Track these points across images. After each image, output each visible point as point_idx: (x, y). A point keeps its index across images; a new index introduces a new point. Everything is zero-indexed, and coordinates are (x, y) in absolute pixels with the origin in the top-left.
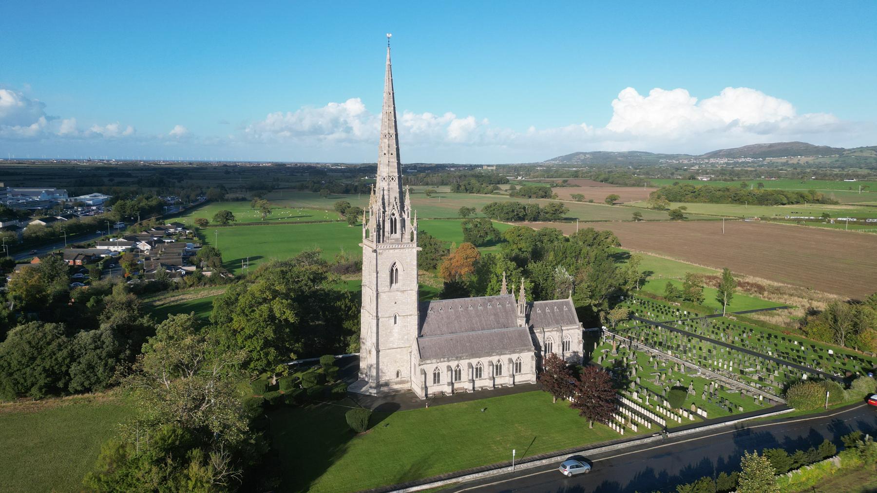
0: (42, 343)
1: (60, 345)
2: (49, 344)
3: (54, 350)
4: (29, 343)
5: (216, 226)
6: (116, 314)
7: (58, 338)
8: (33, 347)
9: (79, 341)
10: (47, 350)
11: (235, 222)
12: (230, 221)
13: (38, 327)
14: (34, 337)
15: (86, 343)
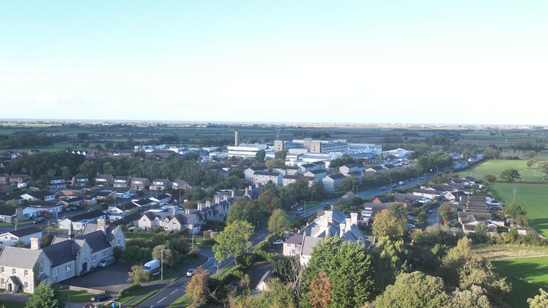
0: (427, 295)
1: (442, 301)
2: (432, 297)
3: (437, 305)
4: (417, 292)
5: (502, 182)
6: (475, 272)
7: (440, 293)
8: (420, 298)
9: (457, 301)
10: (431, 303)
11: (519, 180)
12: (515, 179)
13: (422, 278)
14: (420, 288)
15: (465, 305)
